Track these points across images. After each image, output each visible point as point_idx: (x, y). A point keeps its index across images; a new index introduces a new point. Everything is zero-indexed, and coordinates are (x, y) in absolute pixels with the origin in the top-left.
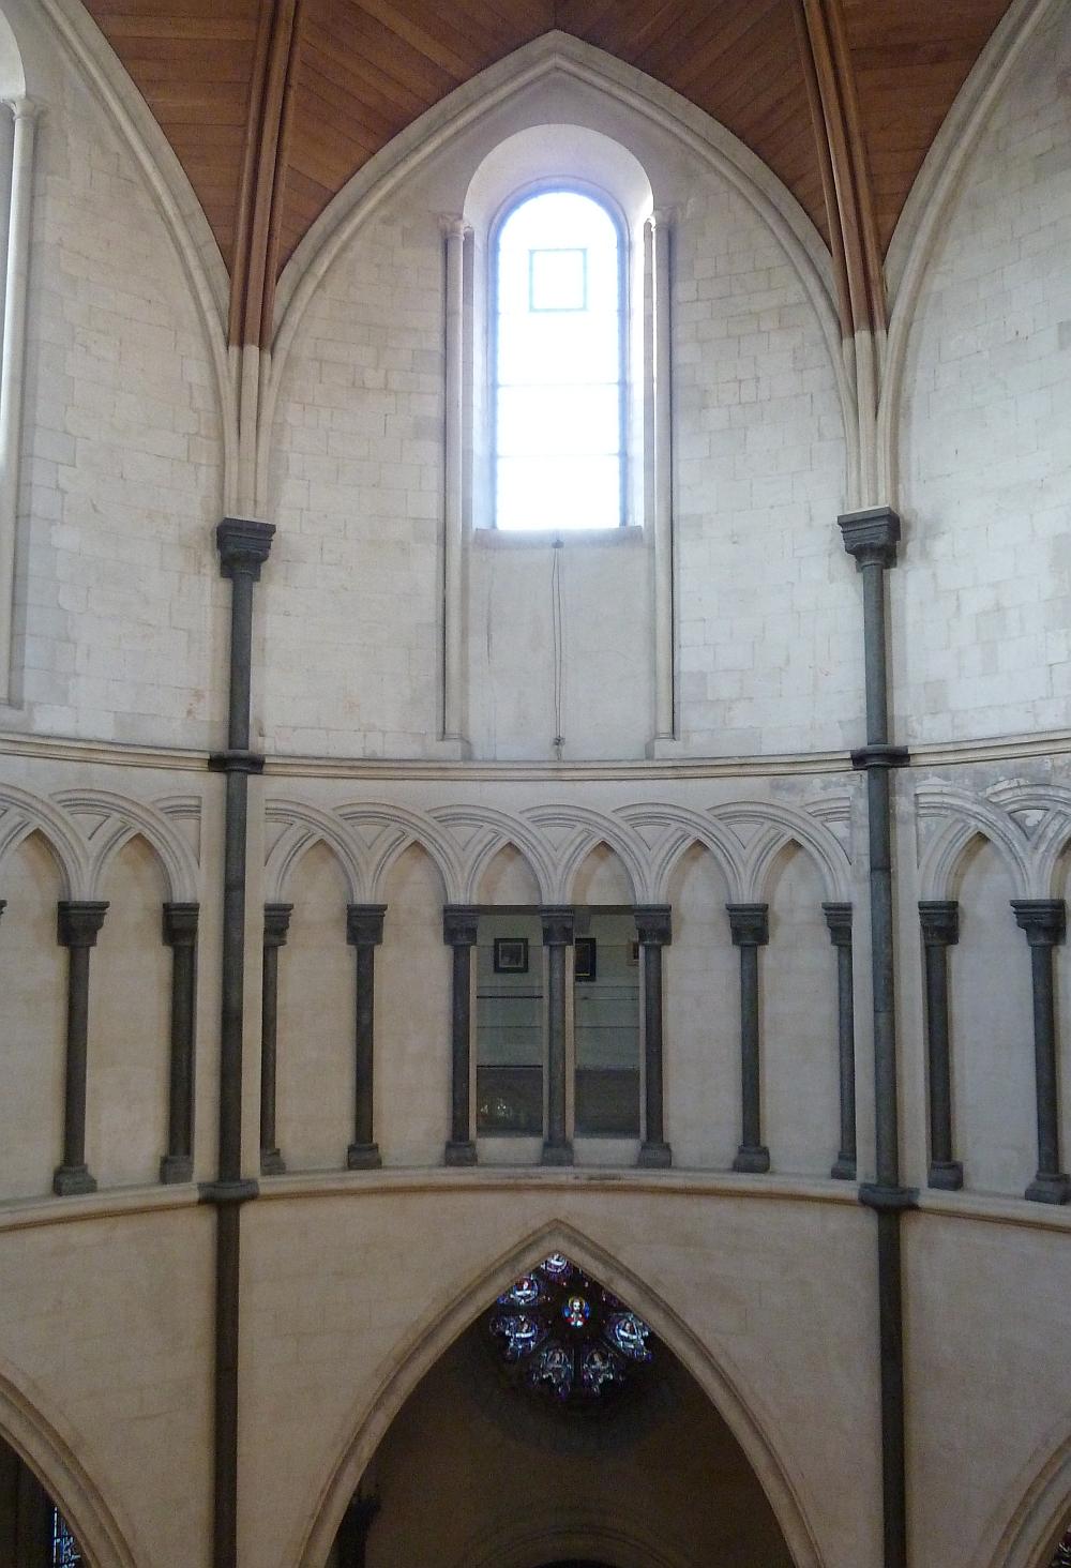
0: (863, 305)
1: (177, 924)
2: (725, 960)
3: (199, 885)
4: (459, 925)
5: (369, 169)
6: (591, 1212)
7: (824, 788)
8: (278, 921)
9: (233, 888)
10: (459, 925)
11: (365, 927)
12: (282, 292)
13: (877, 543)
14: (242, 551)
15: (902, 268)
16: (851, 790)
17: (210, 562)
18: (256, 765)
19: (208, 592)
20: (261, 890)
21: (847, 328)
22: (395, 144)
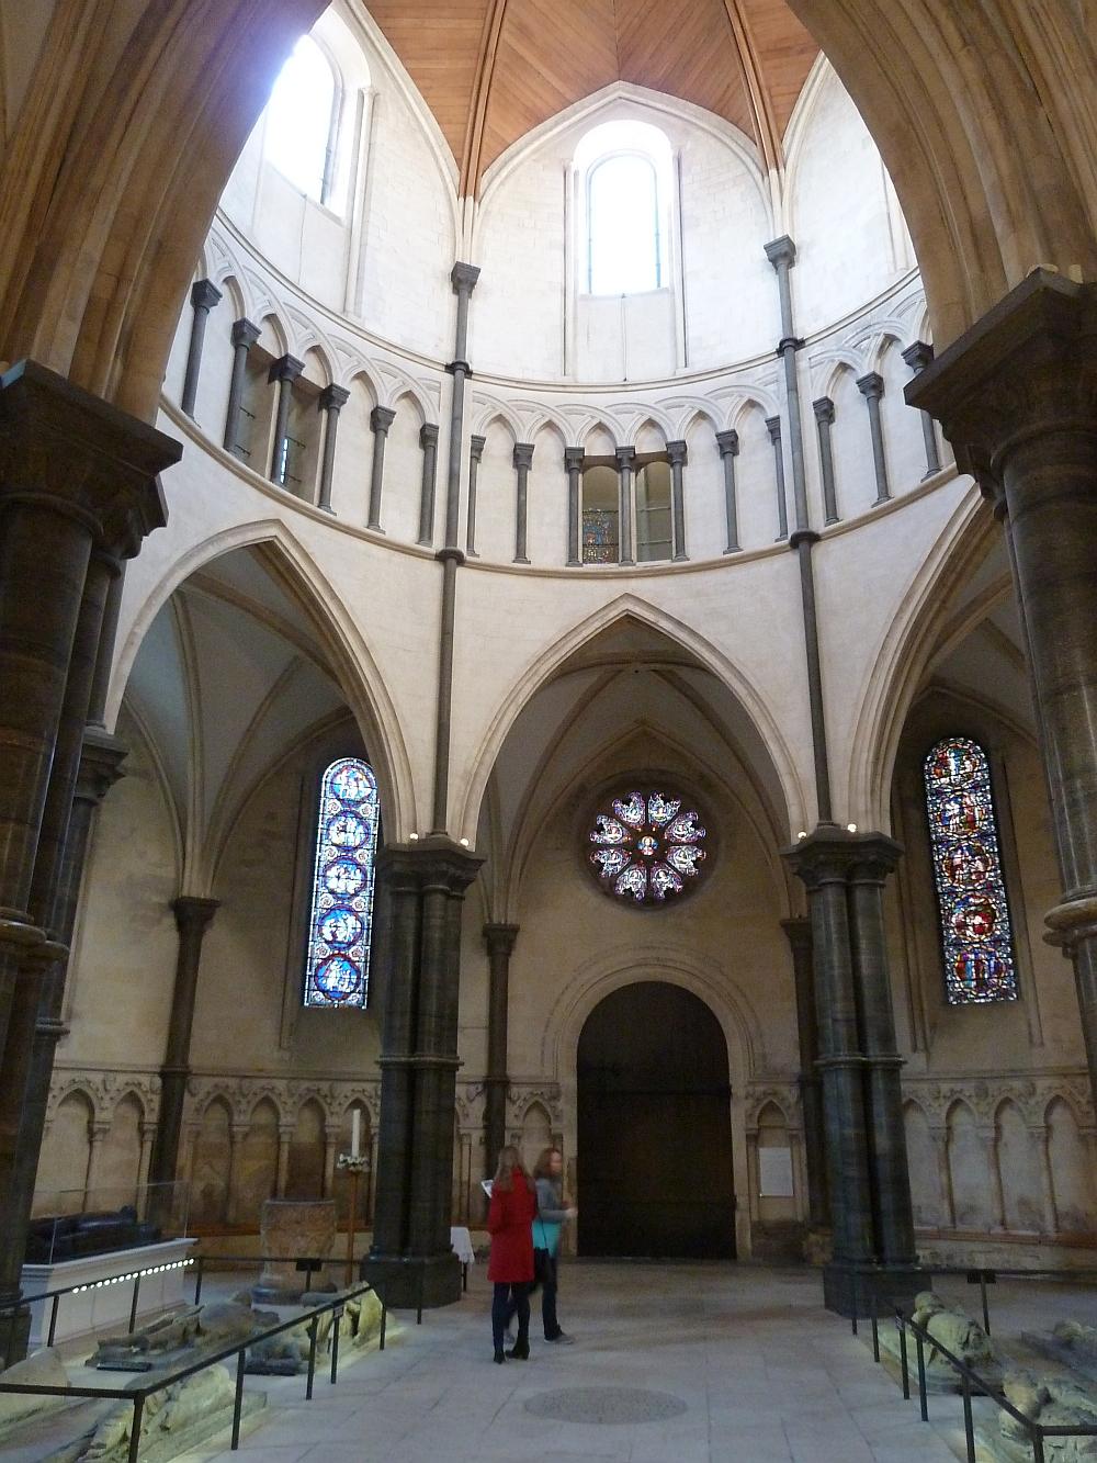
0: (772, 159)
1: (427, 432)
2: (716, 467)
3: (440, 418)
4: (575, 462)
5: (527, 136)
6: (644, 588)
7: (764, 370)
8: (478, 444)
9: (456, 420)
10: (575, 462)
11: (522, 457)
12: (484, 181)
13: (783, 255)
14: (463, 280)
15: (792, 144)
16: (777, 367)
17: (448, 287)
18: (469, 373)
19: (448, 299)
20: (470, 428)
21: (765, 172)
22: (540, 127)
